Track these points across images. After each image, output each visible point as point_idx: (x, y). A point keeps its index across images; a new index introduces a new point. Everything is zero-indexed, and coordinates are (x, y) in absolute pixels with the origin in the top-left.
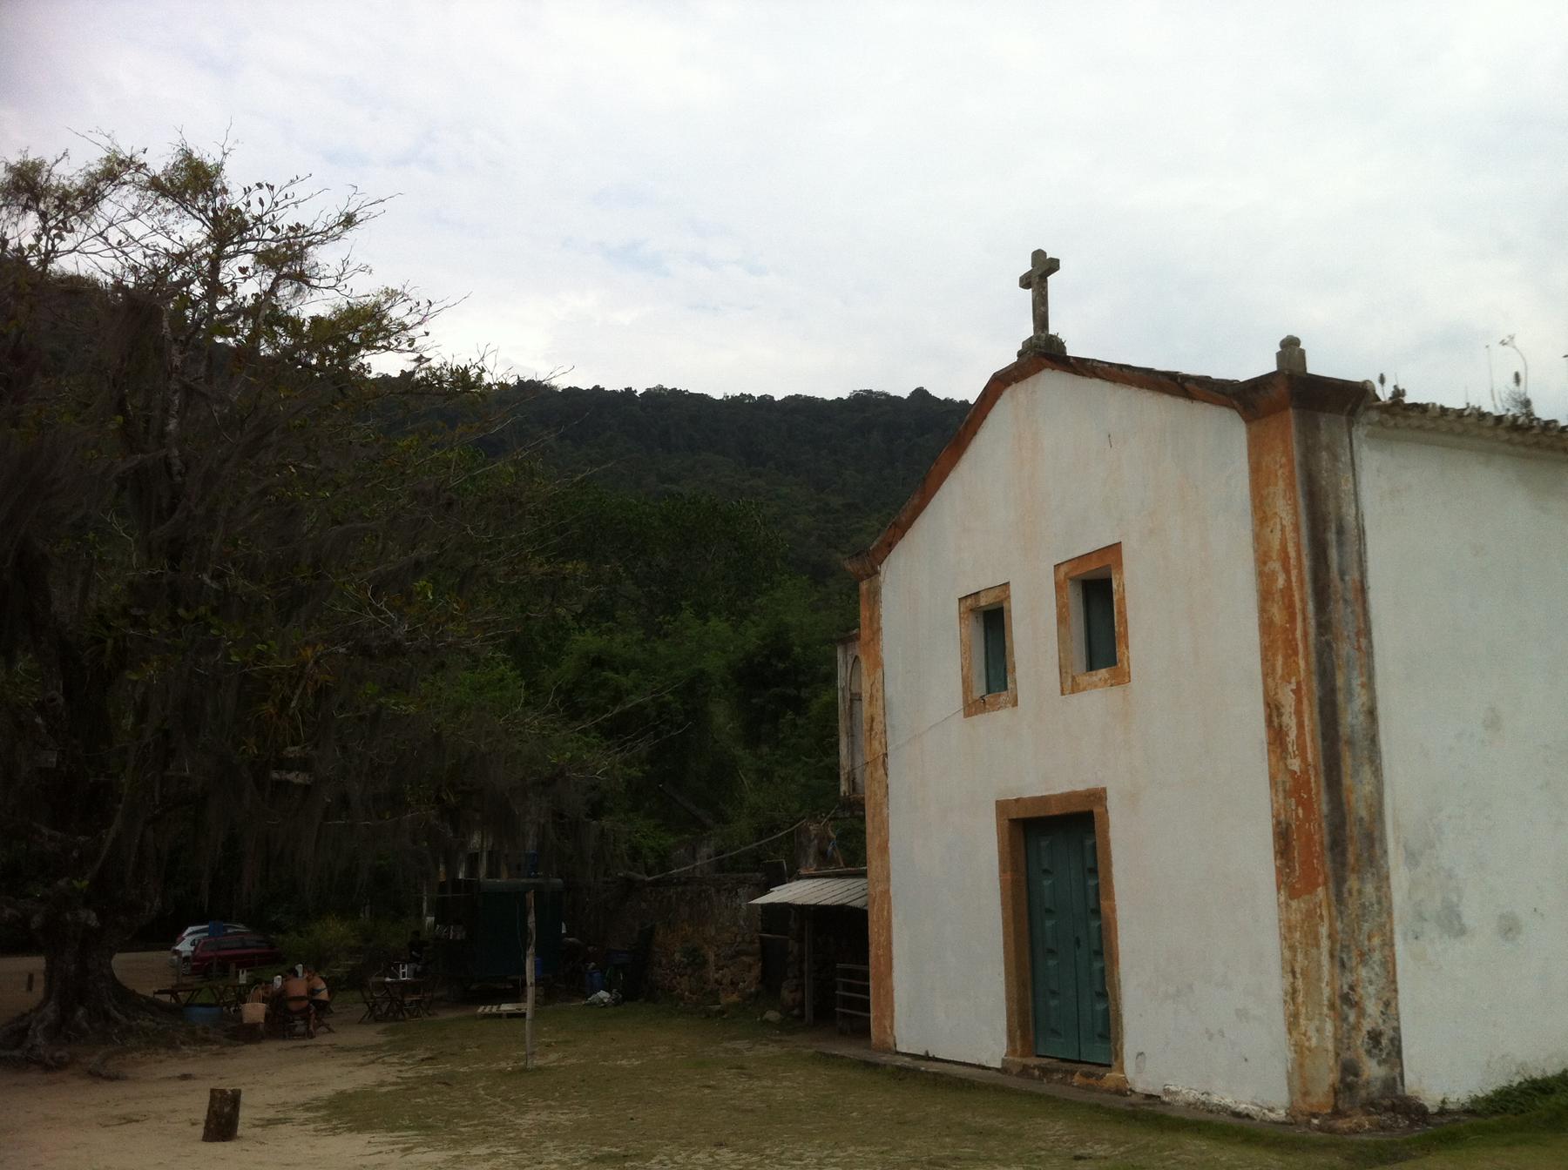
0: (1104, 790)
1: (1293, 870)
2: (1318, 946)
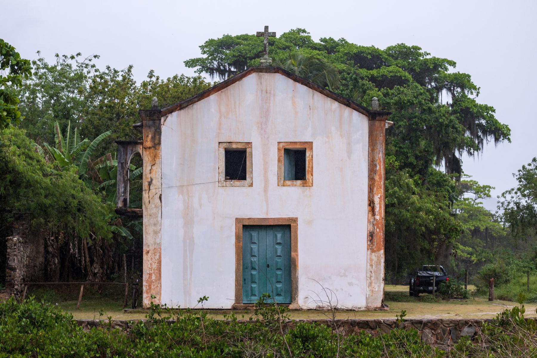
0: (297, 218)
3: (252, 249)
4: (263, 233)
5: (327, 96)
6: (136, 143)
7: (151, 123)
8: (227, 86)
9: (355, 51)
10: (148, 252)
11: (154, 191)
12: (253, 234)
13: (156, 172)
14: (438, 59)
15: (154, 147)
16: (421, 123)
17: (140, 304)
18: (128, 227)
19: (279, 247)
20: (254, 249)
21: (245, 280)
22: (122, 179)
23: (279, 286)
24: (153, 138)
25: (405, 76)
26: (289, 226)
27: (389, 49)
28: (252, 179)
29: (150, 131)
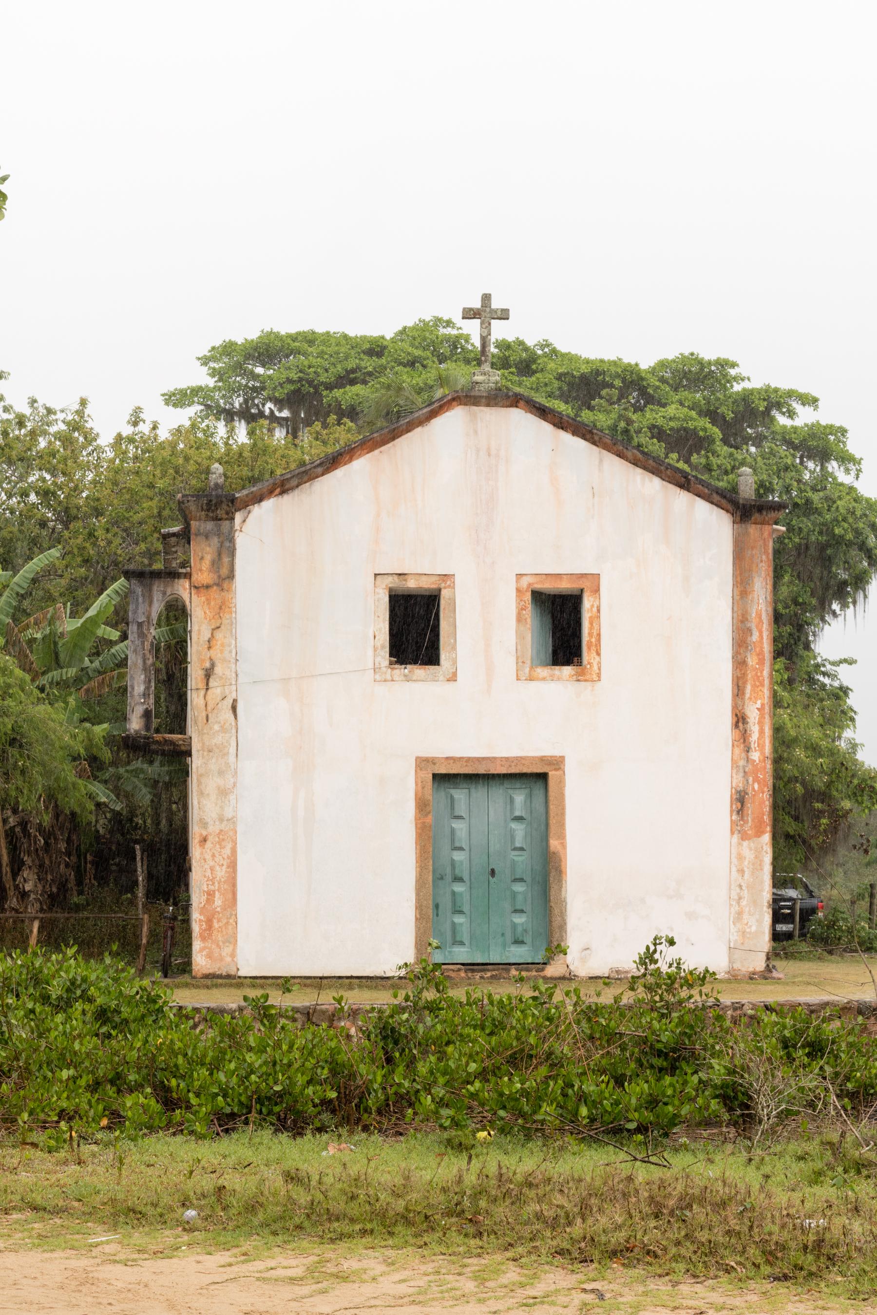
0: (563, 758)
1: (746, 822)
2: (762, 870)
3: (453, 831)
4: (479, 792)
5: (635, 463)
6: (172, 575)
7: (210, 525)
8: (393, 439)
9: (585, 369)
10: (205, 840)
11: (218, 691)
12: (456, 796)
13: (222, 645)
14: (776, 390)
15: (218, 585)
16: (790, 538)
17: (186, 967)
18: (106, 782)
19: (519, 829)
20: (458, 834)
21: (437, 906)
22: (140, 662)
23: (519, 919)
24: (216, 564)
25: (705, 430)
26: (542, 777)
27: (663, 364)
28: (454, 662)
29: (210, 546)
